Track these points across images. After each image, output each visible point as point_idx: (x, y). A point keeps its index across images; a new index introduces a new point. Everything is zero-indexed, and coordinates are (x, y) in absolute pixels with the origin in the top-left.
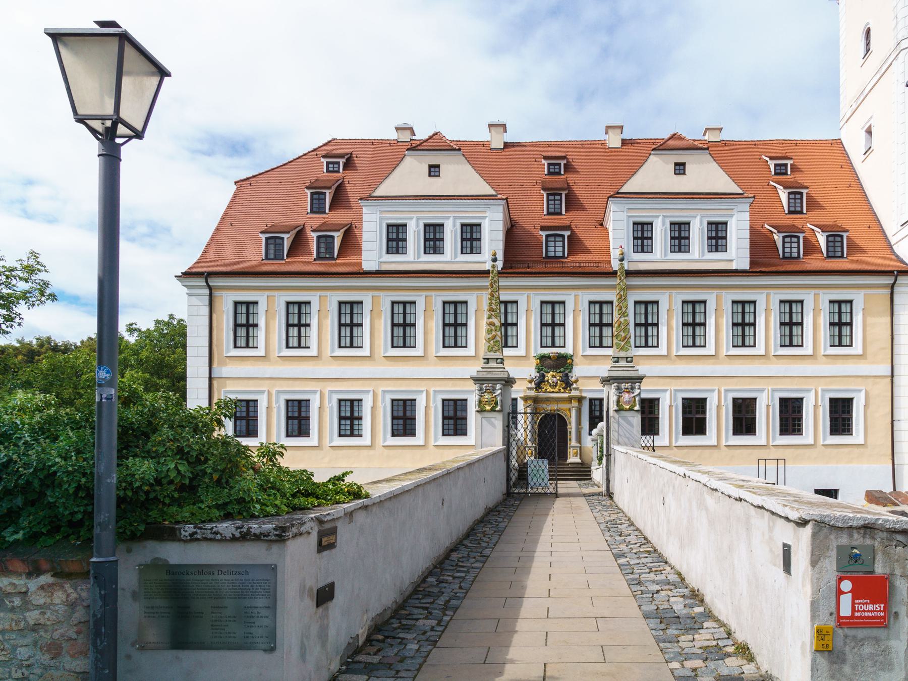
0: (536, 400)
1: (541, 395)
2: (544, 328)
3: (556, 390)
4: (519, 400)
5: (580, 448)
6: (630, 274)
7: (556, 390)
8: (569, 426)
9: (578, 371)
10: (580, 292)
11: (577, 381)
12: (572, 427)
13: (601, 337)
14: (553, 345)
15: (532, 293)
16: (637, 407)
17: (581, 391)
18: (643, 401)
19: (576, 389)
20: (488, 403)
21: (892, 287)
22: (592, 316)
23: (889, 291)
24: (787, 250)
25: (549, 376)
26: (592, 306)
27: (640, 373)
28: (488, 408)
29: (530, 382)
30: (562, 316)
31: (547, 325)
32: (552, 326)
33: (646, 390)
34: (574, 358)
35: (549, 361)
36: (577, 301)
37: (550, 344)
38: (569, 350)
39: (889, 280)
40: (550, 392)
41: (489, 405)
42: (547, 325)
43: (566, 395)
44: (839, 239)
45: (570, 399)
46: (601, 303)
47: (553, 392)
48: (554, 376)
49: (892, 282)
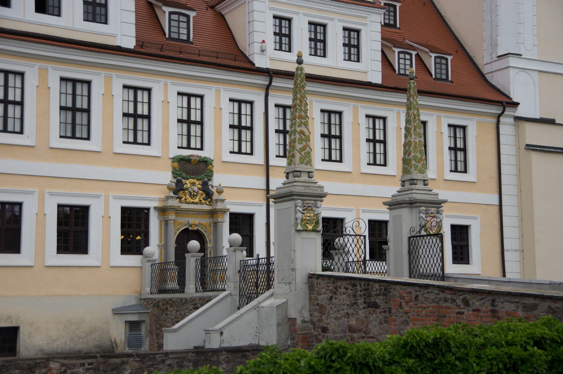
0: (178, 211)
3: (197, 200)
6: (311, 78)
7: (197, 200)
11: (220, 192)
16: (320, 228)
18: (326, 220)
19: (223, 201)
20: (309, 221)
21: (499, 116)
23: (494, 120)
24: (402, 66)
25: (188, 183)
27: (441, 197)
28: (310, 227)
33: (327, 210)
35: (189, 166)
36: (219, 97)
39: (496, 110)
41: (310, 224)
44: (444, 61)
45: (213, 213)
48: (193, 184)
49: (500, 112)
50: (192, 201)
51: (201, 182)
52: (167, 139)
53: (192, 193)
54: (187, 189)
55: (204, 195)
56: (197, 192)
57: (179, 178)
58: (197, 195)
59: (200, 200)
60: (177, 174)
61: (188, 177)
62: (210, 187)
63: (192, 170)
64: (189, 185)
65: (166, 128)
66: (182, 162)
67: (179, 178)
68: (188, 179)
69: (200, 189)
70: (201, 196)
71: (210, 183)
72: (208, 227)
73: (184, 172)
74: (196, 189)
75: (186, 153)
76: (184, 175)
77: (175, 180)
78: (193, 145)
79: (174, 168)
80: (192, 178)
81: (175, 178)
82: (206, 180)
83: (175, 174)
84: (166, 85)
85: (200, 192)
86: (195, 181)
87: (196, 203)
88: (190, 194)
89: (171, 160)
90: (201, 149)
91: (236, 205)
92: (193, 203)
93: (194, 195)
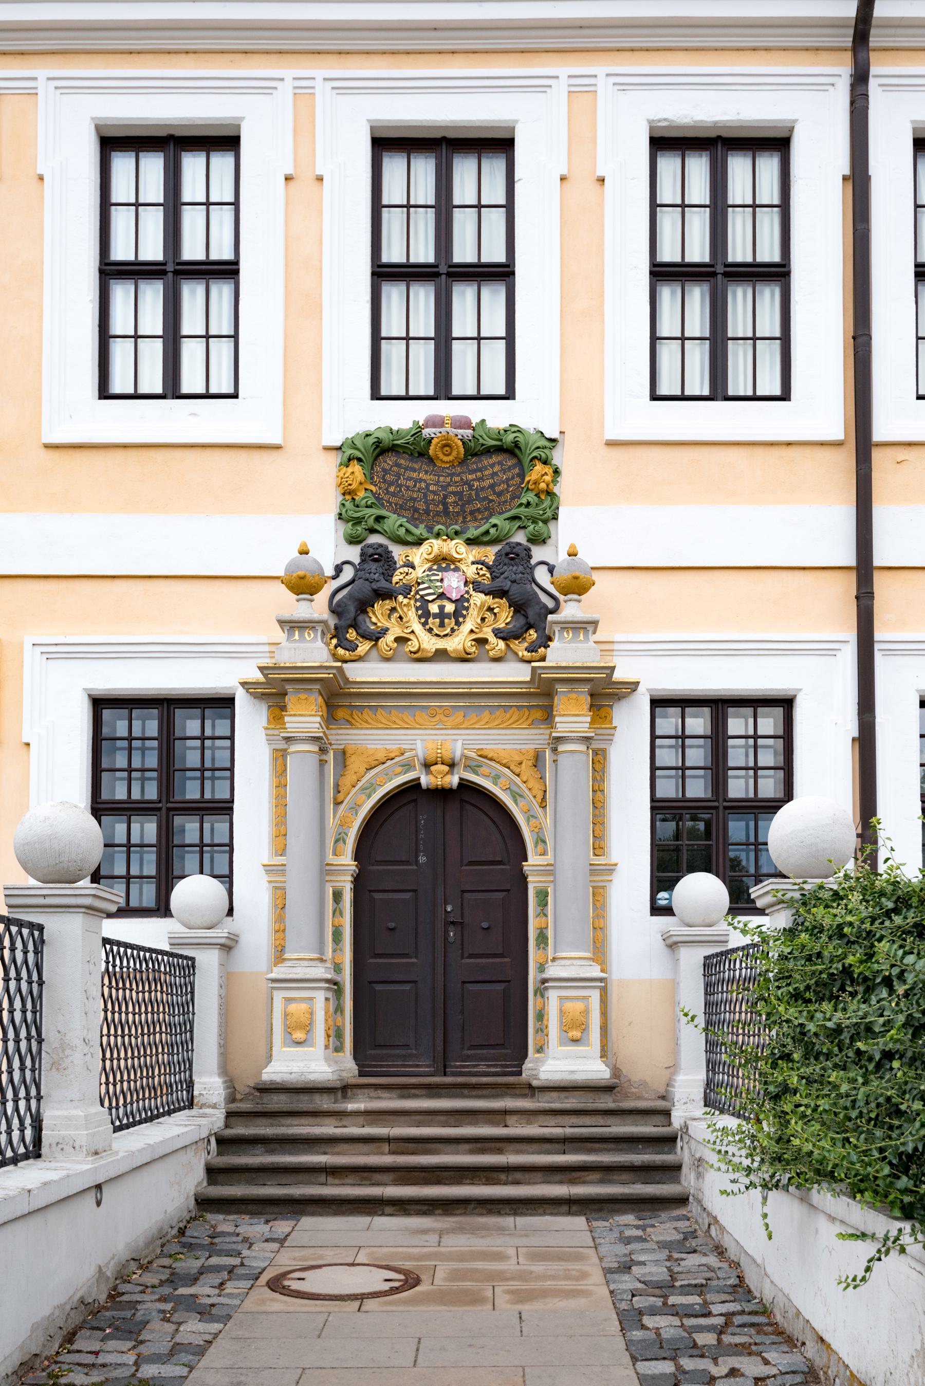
1: (367, 672)
2: (393, 293)
4: (242, 703)
5: (603, 986)
8: (533, 860)
9: (586, 529)
10: (600, 70)
12: (551, 861)
13: (718, 340)
14: (443, 389)
15: (318, 72)
17: (606, 646)
22: (668, 221)
26: (669, 165)
29: (303, 585)
30: (495, 221)
31: (408, 273)
32: (442, 276)
34: (558, 457)
35: (423, 476)
37: (424, 383)
38: (530, 412)
40: (420, 658)
42: (408, 273)
43: (515, 673)
46: (718, 145)
47: (441, 655)
48: (444, 562)
50: (430, 644)
51: (490, 553)
52: (308, 359)
53: (434, 608)
54: (406, 590)
55: (505, 617)
56: (461, 603)
57: (374, 539)
58: (458, 616)
59: (482, 642)
60: (357, 521)
61: (420, 531)
62: (541, 575)
63: (453, 497)
64: (419, 573)
65: (303, 304)
66: (389, 461)
67: (374, 539)
68: (419, 542)
69: (478, 587)
70: (485, 616)
71: (538, 553)
72: (527, 770)
73: (399, 510)
74: (453, 583)
75: (401, 418)
76: (393, 521)
77: (353, 554)
78: (462, 382)
79: (348, 493)
80: (438, 536)
81: (353, 540)
82: (520, 538)
83: (356, 522)
84: (304, 96)
85: (478, 599)
86: (456, 548)
87: (464, 658)
88: (425, 615)
89: (334, 459)
90: (510, 395)
91: (660, 645)
92: (441, 655)
93: (442, 615)
